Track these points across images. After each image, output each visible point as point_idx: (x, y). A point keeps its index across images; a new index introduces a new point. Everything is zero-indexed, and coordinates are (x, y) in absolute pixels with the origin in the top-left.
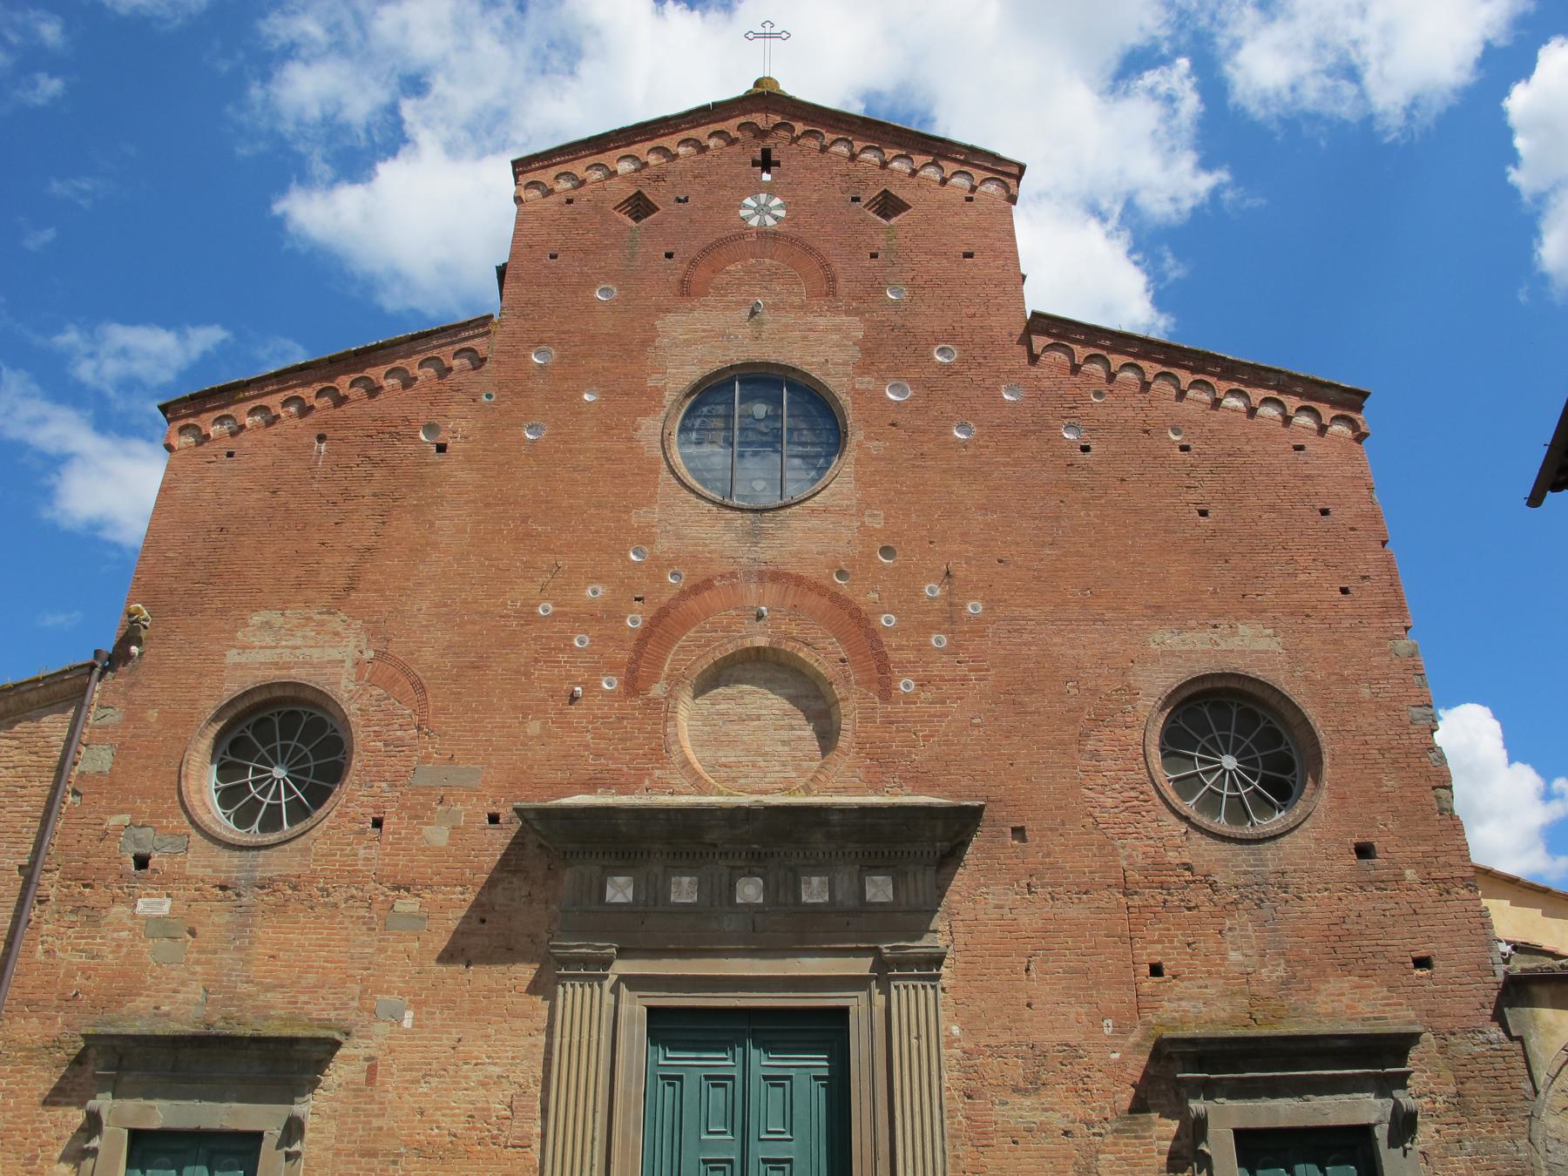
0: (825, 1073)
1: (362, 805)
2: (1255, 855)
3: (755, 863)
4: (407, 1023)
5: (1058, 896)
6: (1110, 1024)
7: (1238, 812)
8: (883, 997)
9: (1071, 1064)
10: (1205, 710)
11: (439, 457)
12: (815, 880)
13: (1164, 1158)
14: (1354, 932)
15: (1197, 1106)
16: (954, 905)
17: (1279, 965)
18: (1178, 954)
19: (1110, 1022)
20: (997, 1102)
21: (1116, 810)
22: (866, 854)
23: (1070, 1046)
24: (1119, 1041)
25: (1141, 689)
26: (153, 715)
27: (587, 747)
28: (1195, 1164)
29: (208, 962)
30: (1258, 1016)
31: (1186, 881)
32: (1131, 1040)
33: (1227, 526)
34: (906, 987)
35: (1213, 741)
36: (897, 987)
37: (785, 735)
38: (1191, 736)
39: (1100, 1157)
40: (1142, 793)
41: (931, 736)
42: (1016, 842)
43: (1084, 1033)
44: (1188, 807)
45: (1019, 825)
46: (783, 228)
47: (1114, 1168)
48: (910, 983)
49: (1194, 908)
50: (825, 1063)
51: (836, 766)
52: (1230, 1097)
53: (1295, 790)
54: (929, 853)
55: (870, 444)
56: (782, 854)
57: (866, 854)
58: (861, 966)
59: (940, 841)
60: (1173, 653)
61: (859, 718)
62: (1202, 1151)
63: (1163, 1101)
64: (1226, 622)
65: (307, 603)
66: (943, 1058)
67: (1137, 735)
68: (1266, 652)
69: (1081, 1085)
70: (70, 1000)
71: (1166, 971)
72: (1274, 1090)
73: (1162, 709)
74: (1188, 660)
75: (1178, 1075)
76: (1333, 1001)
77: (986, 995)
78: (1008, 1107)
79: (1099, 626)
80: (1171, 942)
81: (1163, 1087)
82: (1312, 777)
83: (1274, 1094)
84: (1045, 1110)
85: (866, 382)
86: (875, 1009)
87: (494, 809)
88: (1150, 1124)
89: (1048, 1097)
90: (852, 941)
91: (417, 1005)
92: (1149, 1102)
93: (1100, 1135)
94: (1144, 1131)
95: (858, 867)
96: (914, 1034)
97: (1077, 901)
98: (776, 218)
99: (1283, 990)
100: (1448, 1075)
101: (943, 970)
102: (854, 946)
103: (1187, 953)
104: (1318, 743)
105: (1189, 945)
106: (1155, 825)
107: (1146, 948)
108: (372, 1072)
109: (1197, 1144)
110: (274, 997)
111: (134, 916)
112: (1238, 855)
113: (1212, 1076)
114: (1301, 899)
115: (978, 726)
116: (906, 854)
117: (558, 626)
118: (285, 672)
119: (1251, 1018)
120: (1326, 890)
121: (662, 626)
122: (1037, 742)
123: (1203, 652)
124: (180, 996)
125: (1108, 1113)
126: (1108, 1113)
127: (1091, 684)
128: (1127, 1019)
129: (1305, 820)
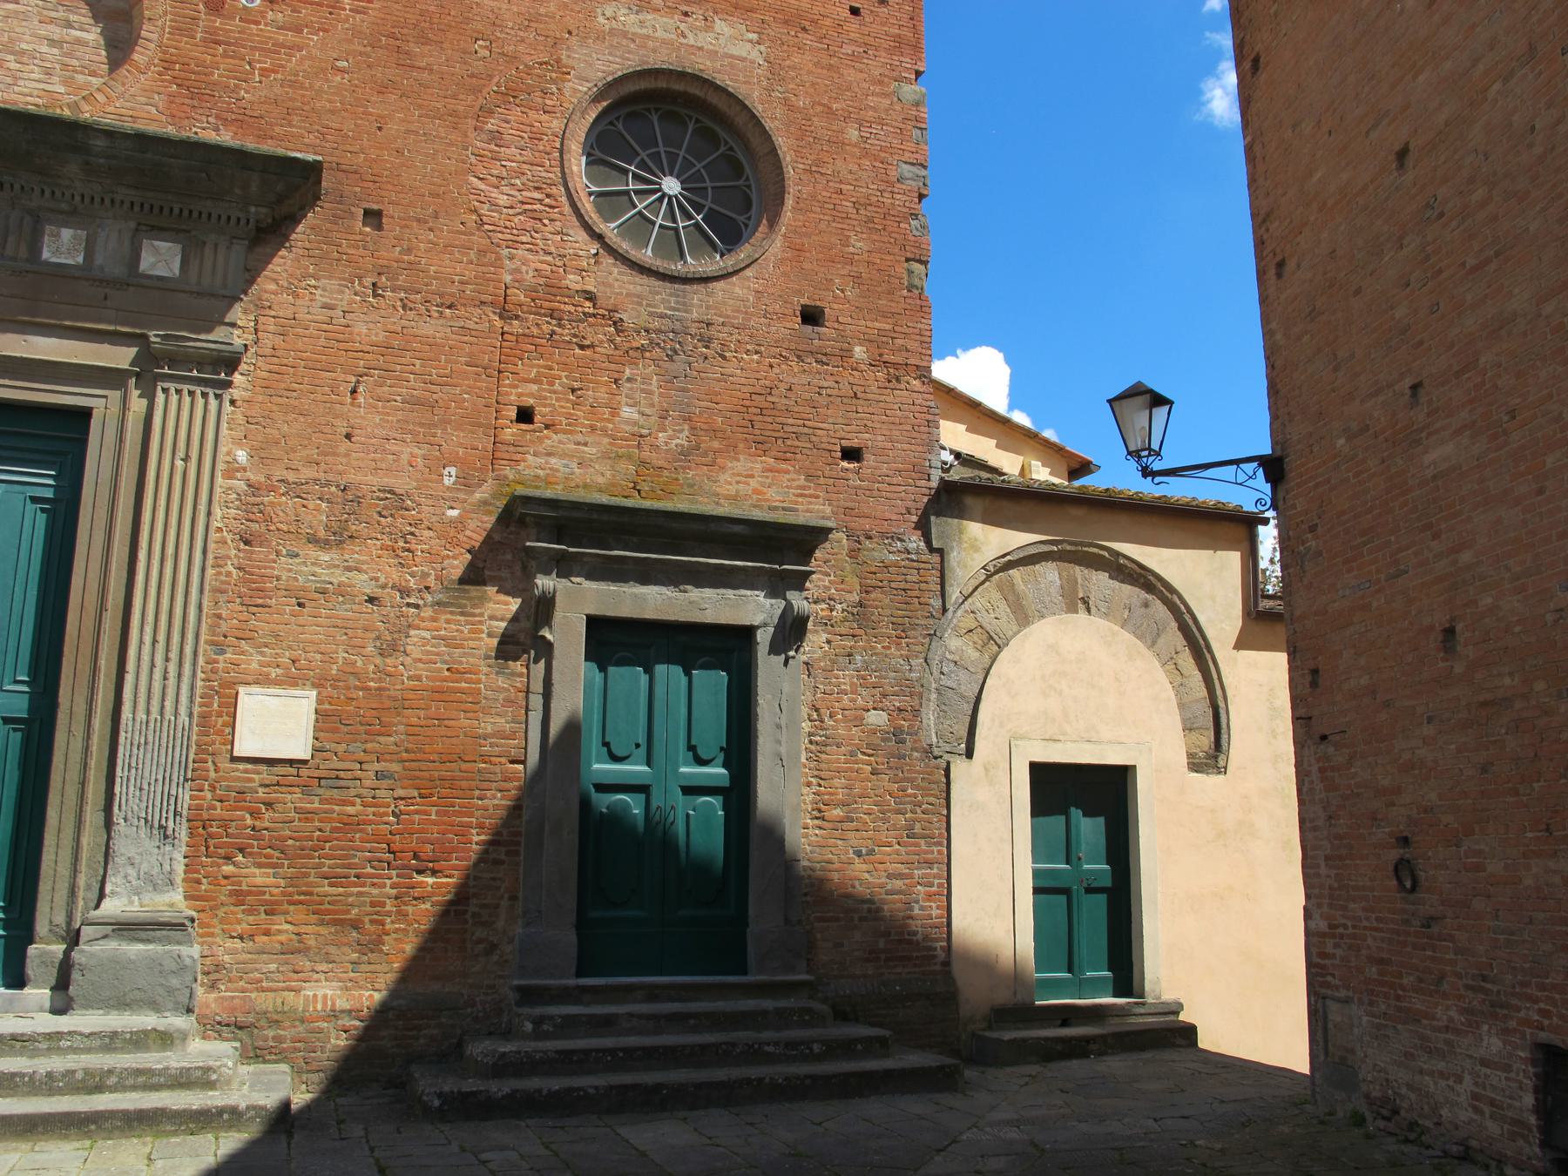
0: (49, 494)
2: (678, 296)
5: (412, 305)
6: (453, 473)
7: (672, 244)
8: (144, 402)
9: (392, 515)
10: (655, 118)
12: (67, 234)
13: (495, 642)
14: (779, 406)
15: (544, 582)
16: (266, 296)
17: (682, 431)
18: (558, 400)
19: (453, 470)
20: (284, 552)
21: (511, 211)
22: (147, 207)
23: (394, 494)
24: (462, 496)
25: (573, 68)
28: (532, 652)
30: (645, 487)
31: (584, 313)
32: (478, 495)
34: (178, 392)
35: (656, 157)
36: (165, 391)
37: (56, 32)
38: (631, 146)
39: (412, 632)
40: (548, 196)
41: (274, 71)
42: (368, 229)
43: (417, 480)
44: (609, 229)
45: (375, 207)
47: (428, 648)
48: (185, 388)
49: (588, 346)
50: (51, 482)
51: (123, 85)
52: (590, 577)
53: (745, 235)
54: (239, 219)
56: (17, 187)
57: (147, 207)
58: (121, 357)
59: (256, 206)
60: (625, 34)
61: (170, 27)
62: (543, 637)
63: (505, 573)
64: (700, 12)
66: (218, 490)
67: (557, 125)
68: (743, 60)
69: (401, 544)
71: (537, 418)
72: (646, 573)
73: (596, 99)
74: (644, 46)
75: (528, 544)
76: (738, 482)
77: (291, 417)
78: (297, 560)
80: (552, 384)
81: (509, 557)
82: (767, 220)
83: (645, 580)
84: (349, 569)
86: (130, 417)
88: (483, 599)
89: (354, 553)
90: (110, 323)
92: (487, 573)
93: (417, 606)
94: (474, 606)
95: (132, 225)
96: (181, 453)
97: (436, 315)
99: (681, 460)
100: (854, 582)
101: (237, 378)
102: (112, 328)
103: (568, 400)
104: (783, 180)
105: (573, 390)
106: (558, 238)
107: (516, 387)
109: (538, 627)
112: (658, 293)
113: (571, 550)
114: (724, 358)
115: (342, 71)
116: (204, 216)
119: (634, 488)
120: (757, 353)
122: (420, 107)
123: (664, 42)
125: (431, 581)
126: (431, 581)
127: (509, 49)
128: (476, 470)
129: (748, 266)
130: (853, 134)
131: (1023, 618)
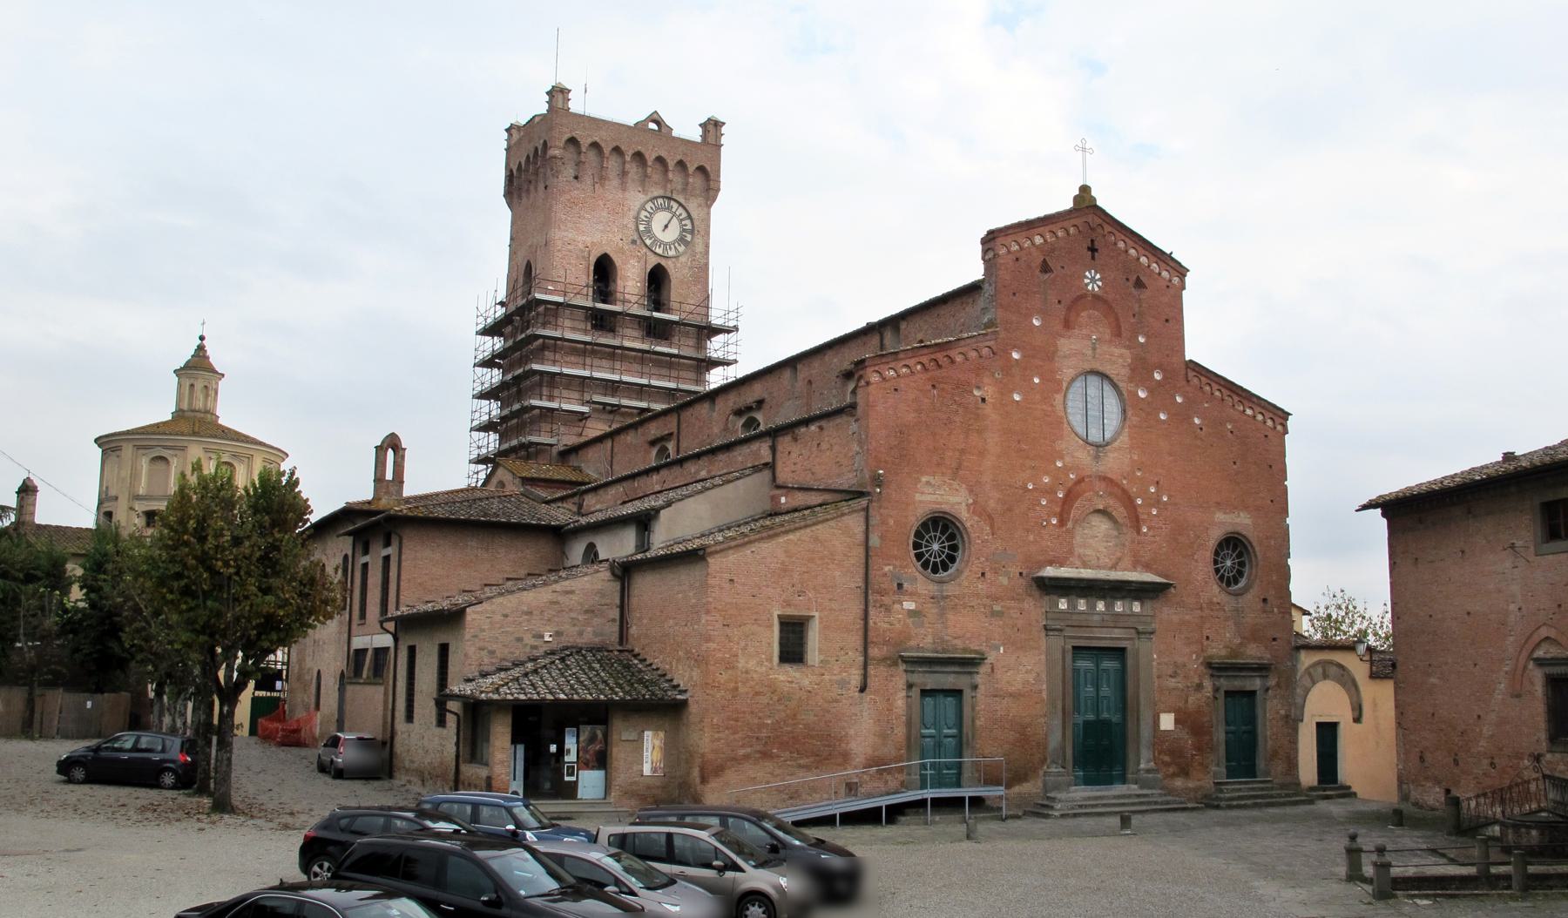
1: (978, 567)
3: (1103, 598)
4: (1002, 651)
11: (981, 405)
26: (891, 522)
27: (1048, 547)
33: (1241, 470)
46: (1100, 294)
70: (886, 643)
85: (1131, 387)
87: (1021, 571)
89: (1179, 679)
91: (1004, 645)
98: (1098, 285)
110: (956, 642)
111: (903, 609)
117: (1036, 494)
118: (938, 506)
121: (1070, 496)
130: (1272, 543)
131: (1314, 683)
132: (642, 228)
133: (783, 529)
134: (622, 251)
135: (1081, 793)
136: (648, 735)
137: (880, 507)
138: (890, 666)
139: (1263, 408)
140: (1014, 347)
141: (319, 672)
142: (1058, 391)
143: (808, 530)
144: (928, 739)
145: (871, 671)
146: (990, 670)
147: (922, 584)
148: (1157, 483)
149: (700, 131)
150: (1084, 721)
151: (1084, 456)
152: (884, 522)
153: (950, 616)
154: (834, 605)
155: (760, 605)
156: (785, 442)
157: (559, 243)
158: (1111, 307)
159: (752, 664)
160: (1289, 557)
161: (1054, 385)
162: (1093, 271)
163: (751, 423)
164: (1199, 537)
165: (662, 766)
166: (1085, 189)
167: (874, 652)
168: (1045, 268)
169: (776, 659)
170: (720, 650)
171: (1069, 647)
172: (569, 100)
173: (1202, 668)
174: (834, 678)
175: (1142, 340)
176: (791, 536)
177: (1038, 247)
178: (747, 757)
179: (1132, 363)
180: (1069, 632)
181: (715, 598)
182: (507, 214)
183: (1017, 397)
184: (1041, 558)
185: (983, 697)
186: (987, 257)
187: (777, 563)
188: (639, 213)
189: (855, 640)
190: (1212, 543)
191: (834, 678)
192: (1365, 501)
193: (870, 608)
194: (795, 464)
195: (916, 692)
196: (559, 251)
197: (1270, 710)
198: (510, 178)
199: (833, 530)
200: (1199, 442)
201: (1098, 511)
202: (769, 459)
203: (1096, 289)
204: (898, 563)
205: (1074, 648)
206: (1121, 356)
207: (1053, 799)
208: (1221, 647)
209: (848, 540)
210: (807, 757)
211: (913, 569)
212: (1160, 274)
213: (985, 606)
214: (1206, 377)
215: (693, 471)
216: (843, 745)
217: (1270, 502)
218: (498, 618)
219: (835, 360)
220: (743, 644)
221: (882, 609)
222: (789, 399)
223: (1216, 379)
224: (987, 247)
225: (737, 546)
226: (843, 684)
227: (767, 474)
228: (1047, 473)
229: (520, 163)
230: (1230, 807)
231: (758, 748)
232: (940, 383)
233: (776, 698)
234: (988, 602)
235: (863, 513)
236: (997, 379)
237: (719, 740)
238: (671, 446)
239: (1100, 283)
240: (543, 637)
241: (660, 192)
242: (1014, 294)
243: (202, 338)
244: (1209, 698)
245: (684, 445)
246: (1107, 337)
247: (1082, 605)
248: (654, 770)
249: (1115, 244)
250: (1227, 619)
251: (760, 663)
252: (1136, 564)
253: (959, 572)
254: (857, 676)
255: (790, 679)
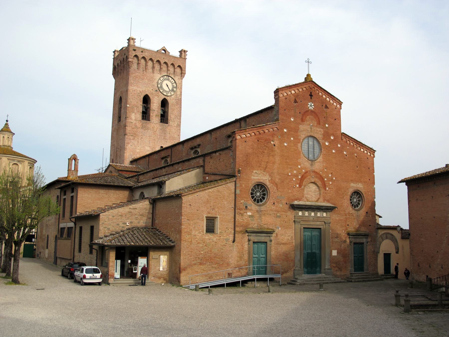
4: (280, 229)
11: (274, 147)
27: (295, 194)
29: (257, 221)
55: (324, 152)
65: (261, 170)
70: (242, 226)
79: (346, 182)
85: (323, 141)
91: (281, 227)
108: (277, 235)
110: (265, 226)
111: (247, 215)
121: (303, 178)
124: (255, 225)
131: (383, 240)
132: (159, 86)
133: (207, 188)
134: (152, 94)
135: (306, 277)
136: (162, 257)
137: (240, 181)
138: (243, 234)
139: (367, 149)
140: (285, 128)
141: (48, 235)
142: (299, 143)
143: (216, 188)
144: (255, 258)
145: (236, 235)
146: (276, 235)
147: (254, 206)
148: (332, 173)
149: (179, 54)
150: (307, 253)
151: (307, 164)
152: (241, 186)
153: (263, 217)
154: (224, 213)
155: (200, 213)
156: (208, 159)
157: (131, 91)
158: (317, 115)
159: (197, 233)
160: (375, 198)
161: (297, 140)
162: (311, 103)
163: (196, 152)
164: (345, 191)
165: (166, 267)
166: (308, 75)
167: (237, 229)
168: (296, 101)
169: (205, 231)
170: (186, 228)
171: (302, 228)
172: (135, 42)
173: (346, 235)
174: (224, 238)
175: (327, 126)
176: (210, 190)
177: (293, 95)
178: (195, 264)
179: (324, 133)
180: (302, 223)
181: (184, 211)
182: (113, 80)
183: (285, 144)
184: (293, 198)
185: (274, 244)
186: (276, 98)
187: (205, 199)
188: (158, 81)
189: (231, 225)
190: (350, 194)
191: (224, 238)
192: (400, 180)
193: (236, 215)
194: (211, 166)
195: (251, 242)
196: (131, 93)
197: (368, 249)
198: (114, 68)
199: (224, 188)
200: (345, 160)
201: (312, 183)
202: (202, 164)
203: (312, 109)
204: (245, 199)
205: (304, 228)
206: (320, 131)
207: (297, 278)
208: (352, 228)
209: (229, 192)
210: (215, 264)
211: (250, 202)
212: (333, 104)
213: (274, 214)
214: (348, 138)
215: (177, 168)
216: (227, 260)
217: (368, 180)
218: (111, 217)
219: (225, 131)
220: (193, 226)
221: (240, 215)
222: (209, 144)
223: (351, 139)
224: (276, 94)
225: (192, 193)
226: (227, 240)
227: (202, 169)
228: (295, 170)
229: (118, 63)
230: (355, 282)
231: (199, 261)
232: (260, 139)
233: (205, 245)
234: (275, 213)
235: (234, 183)
236: (279, 138)
237: (186, 258)
238: (169, 160)
239: (313, 107)
240: (126, 224)
241: (166, 74)
242: (285, 110)
243: (7, 121)
244: (348, 245)
245: (173, 159)
246: (316, 125)
247: (307, 214)
248: (164, 269)
249: (319, 94)
250: (354, 219)
251: (200, 233)
252: (324, 200)
253: (266, 203)
254: (232, 237)
255: (209, 238)
